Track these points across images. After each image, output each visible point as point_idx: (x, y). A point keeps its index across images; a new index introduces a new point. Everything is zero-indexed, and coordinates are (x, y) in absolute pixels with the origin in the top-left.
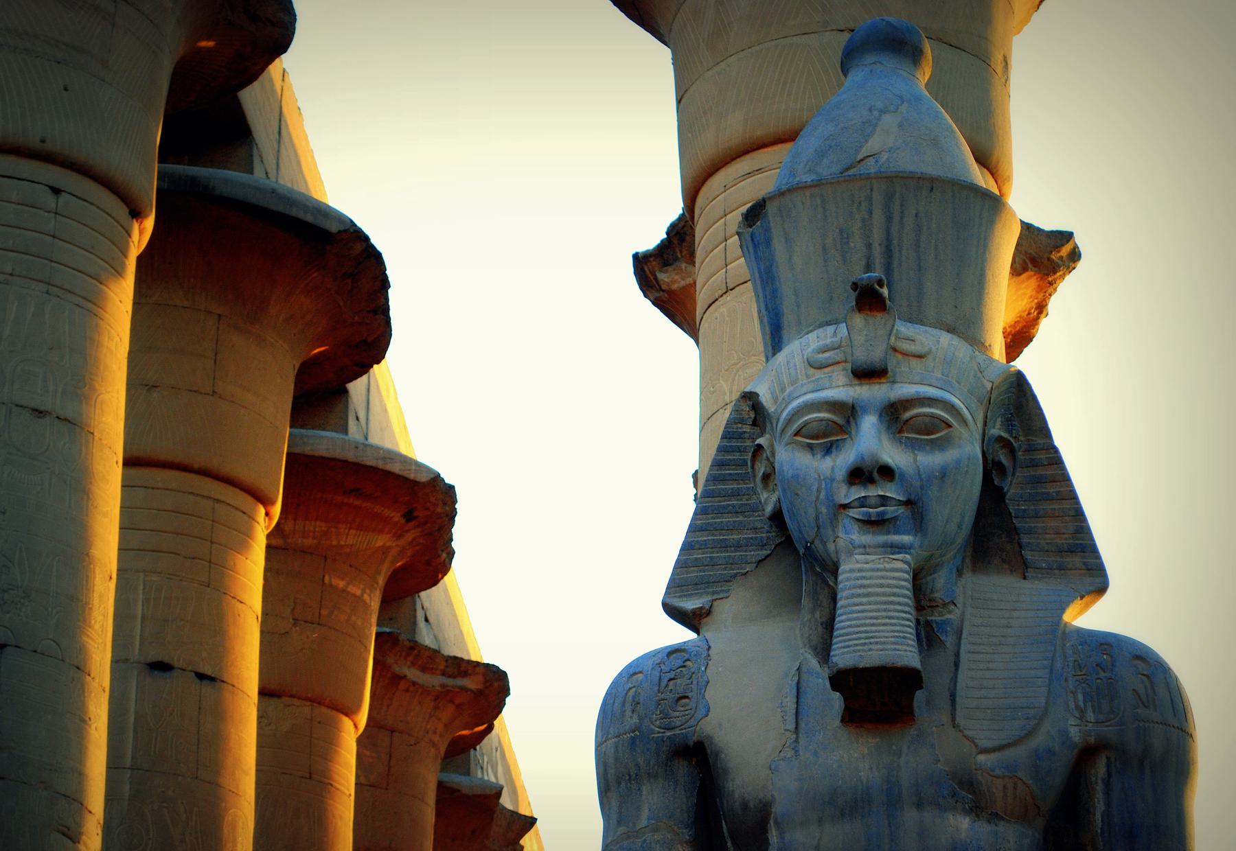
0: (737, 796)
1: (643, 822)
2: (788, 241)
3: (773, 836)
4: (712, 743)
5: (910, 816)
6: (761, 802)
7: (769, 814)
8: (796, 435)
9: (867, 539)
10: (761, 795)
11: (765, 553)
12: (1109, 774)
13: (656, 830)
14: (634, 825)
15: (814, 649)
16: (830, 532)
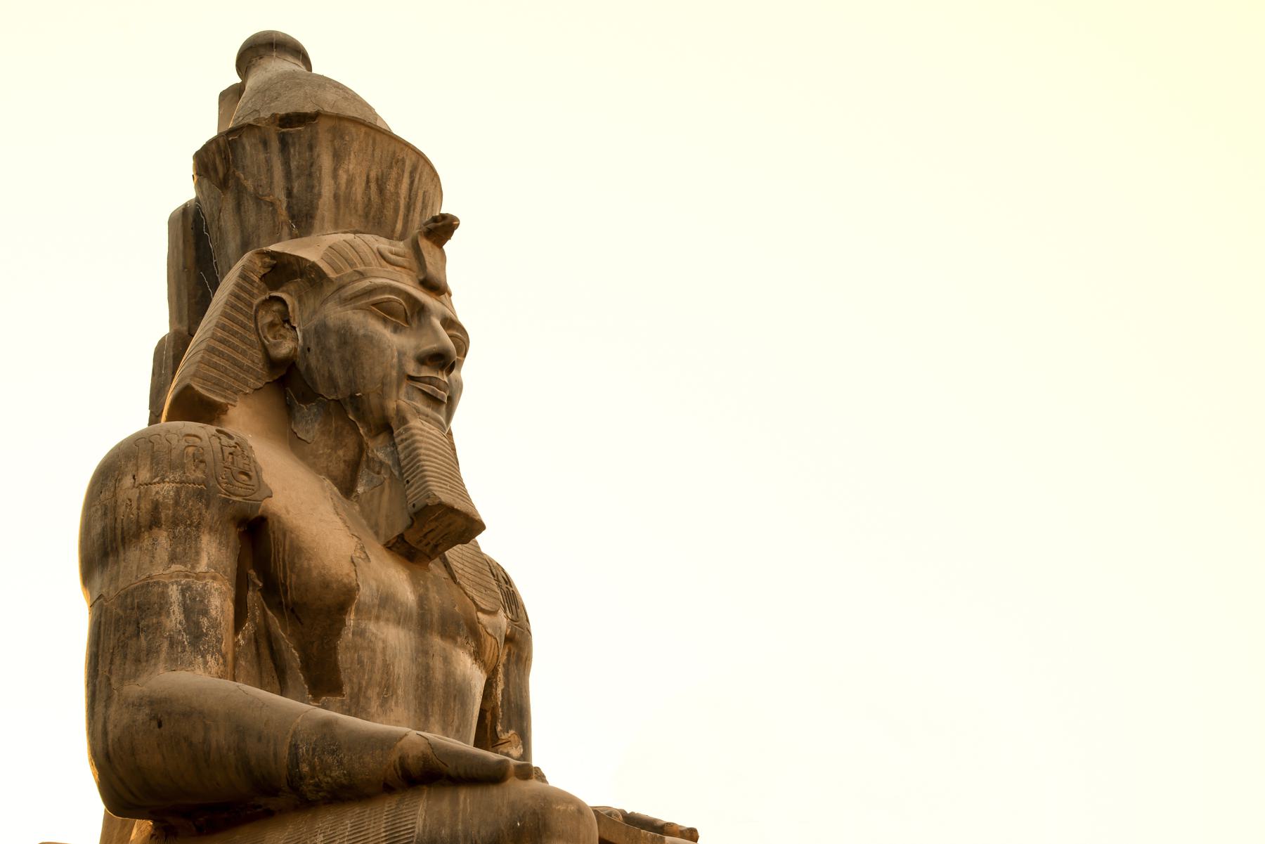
0: (315, 573)
1: (202, 567)
2: (338, 157)
3: (351, 619)
4: (279, 522)
5: (437, 642)
6: (345, 585)
7: (354, 599)
8: (373, 305)
9: (429, 411)
10: (346, 581)
11: (260, 385)
12: (508, 660)
13: (214, 578)
14: (193, 567)
15: (335, 480)
16: (394, 393)
